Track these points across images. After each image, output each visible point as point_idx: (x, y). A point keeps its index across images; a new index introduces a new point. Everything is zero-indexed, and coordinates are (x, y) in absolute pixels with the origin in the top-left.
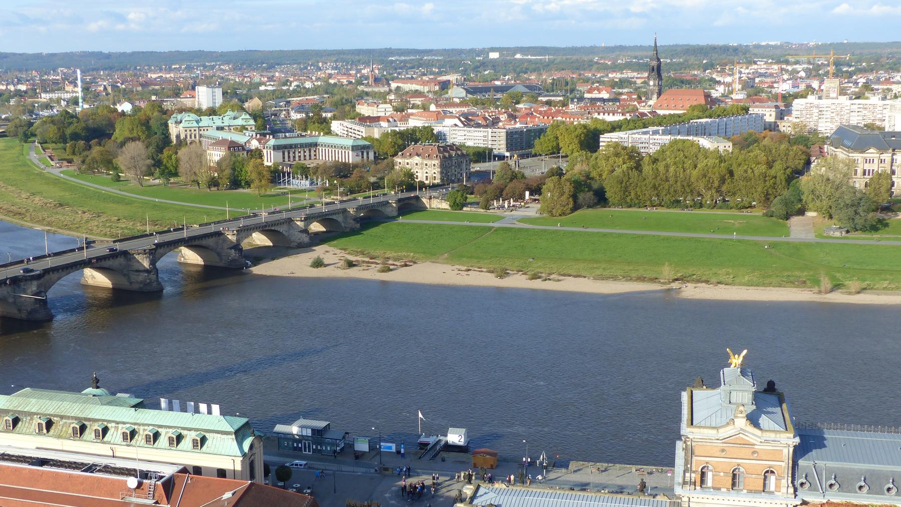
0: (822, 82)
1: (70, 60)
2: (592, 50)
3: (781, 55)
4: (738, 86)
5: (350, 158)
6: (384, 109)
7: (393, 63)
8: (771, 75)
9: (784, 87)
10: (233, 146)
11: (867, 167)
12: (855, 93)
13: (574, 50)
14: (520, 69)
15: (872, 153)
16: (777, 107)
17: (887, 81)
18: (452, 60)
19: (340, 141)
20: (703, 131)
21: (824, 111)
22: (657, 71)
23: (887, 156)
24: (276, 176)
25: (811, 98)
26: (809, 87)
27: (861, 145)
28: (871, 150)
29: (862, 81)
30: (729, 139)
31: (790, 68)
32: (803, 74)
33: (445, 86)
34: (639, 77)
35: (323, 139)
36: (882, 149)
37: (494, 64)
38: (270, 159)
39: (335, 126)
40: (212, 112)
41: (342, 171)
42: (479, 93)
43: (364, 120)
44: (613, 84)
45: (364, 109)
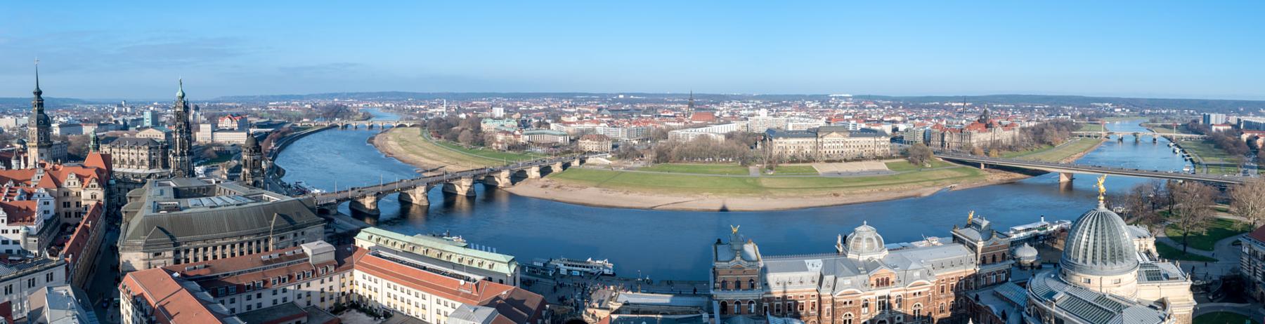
1: (441, 96)
2: (664, 95)
3: (743, 99)
5: (560, 139)
6: (574, 119)
7: (576, 99)
10: (507, 133)
13: (656, 95)
14: (632, 102)
18: (603, 98)
19: (556, 132)
21: (762, 120)
22: (691, 105)
24: (524, 146)
33: (600, 109)
34: (685, 108)
35: (547, 131)
36: (785, 137)
37: (621, 100)
38: (523, 139)
39: (553, 126)
40: (499, 119)
41: (556, 146)
42: (615, 113)
43: (565, 124)
44: (673, 110)
45: (565, 119)
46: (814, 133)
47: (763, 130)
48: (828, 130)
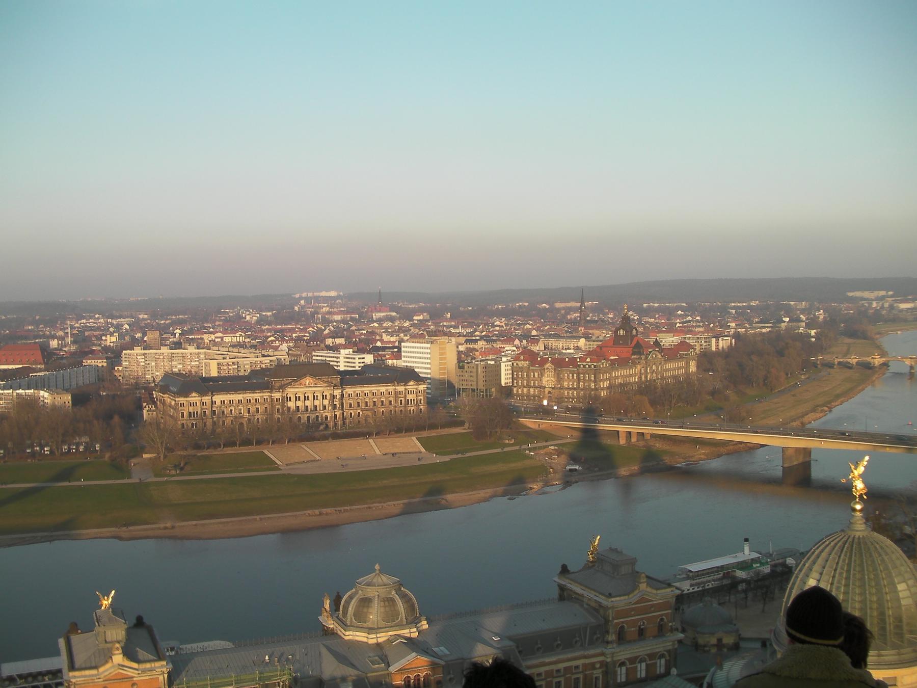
0: (144, 334)
4: (69, 340)
8: (99, 328)
9: (111, 340)
11: (191, 409)
12: (174, 343)
15: (194, 398)
16: (107, 358)
17: (199, 332)
20: (40, 384)
23: (207, 399)
25: (138, 350)
26: (133, 338)
27: (184, 391)
28: (194, 394)
29: (178, 331)
30: (67, 391)
31: (114, 322)
32: (127, 327)
36: (202, 393)
46: (257, 380)
47: (155, 373)
48: (294, 371)
